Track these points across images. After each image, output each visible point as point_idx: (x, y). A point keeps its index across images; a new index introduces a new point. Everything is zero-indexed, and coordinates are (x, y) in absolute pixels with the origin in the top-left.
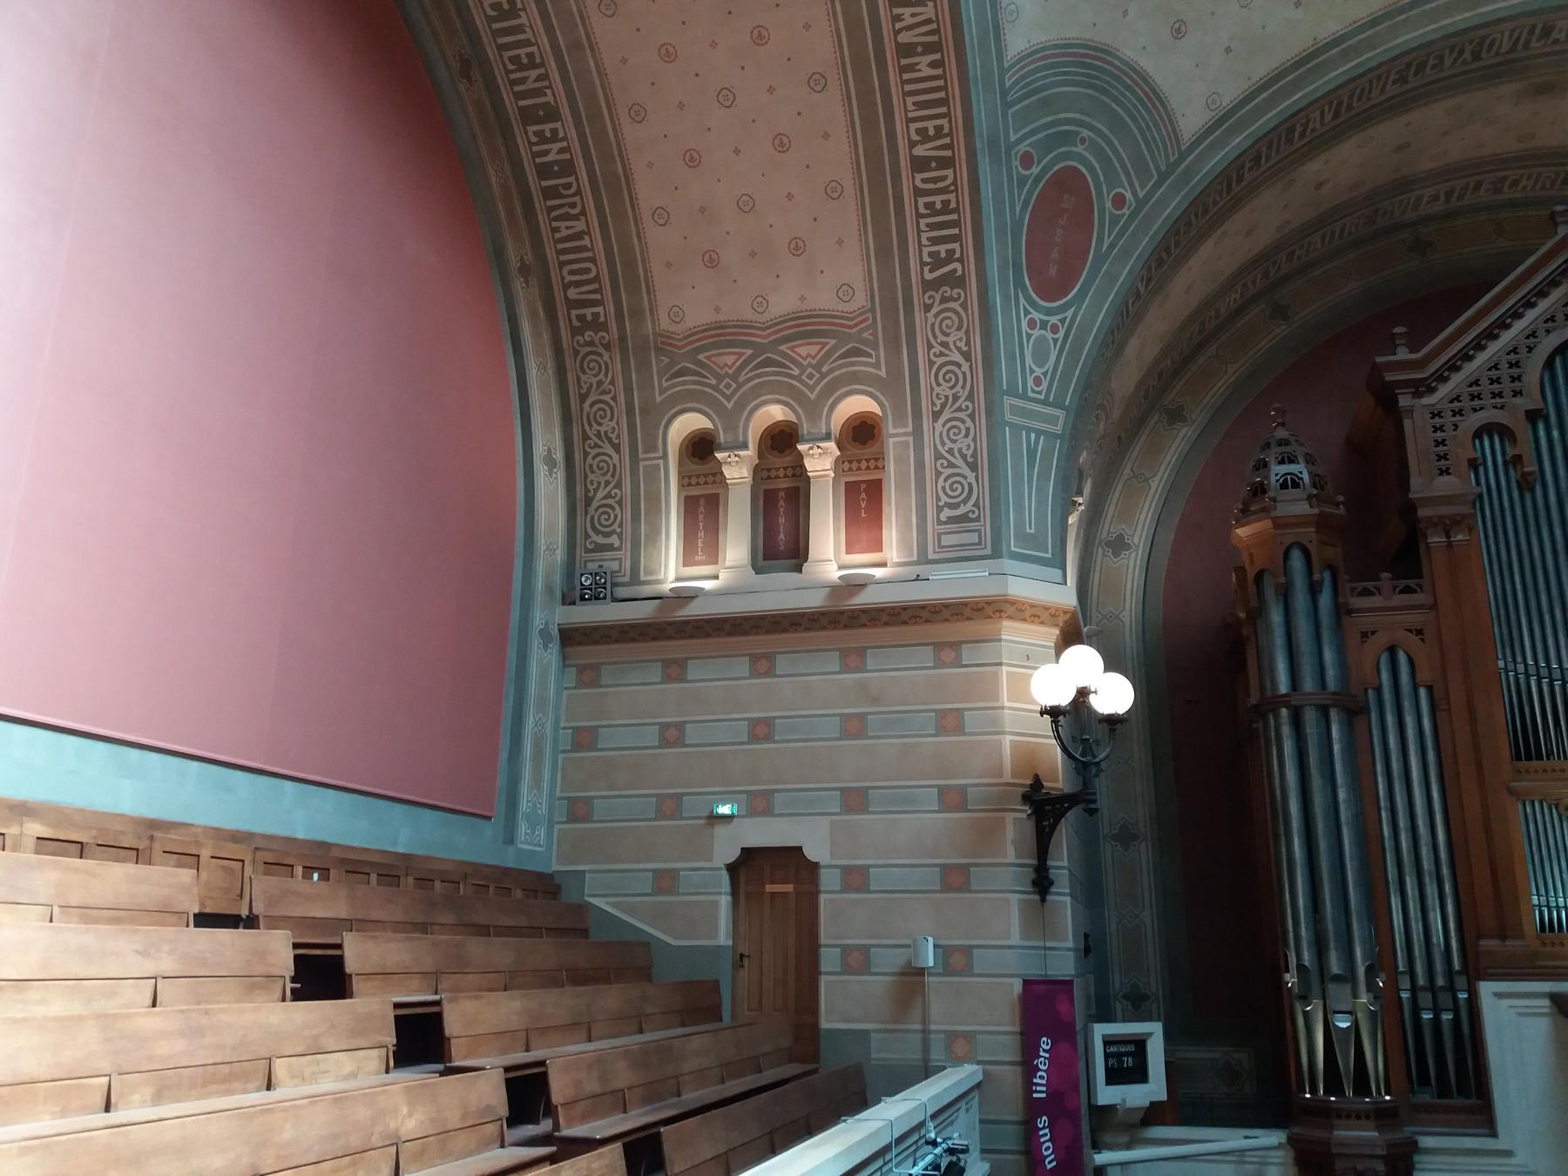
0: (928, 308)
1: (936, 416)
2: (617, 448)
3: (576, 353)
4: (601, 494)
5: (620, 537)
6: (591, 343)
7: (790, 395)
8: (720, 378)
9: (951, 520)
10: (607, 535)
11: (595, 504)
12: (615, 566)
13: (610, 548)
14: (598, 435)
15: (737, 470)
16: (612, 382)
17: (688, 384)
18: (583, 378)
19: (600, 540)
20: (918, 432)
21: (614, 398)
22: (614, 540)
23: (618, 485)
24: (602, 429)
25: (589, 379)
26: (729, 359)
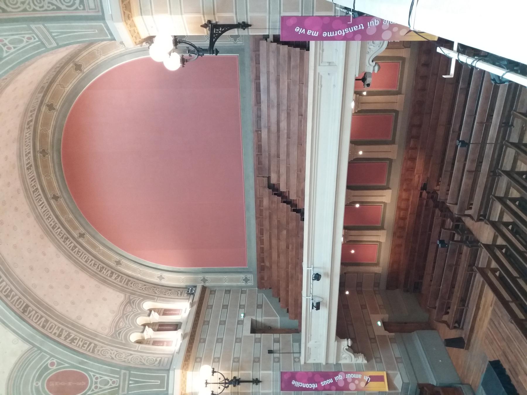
0: (131, 287)
1: (156, 293)
2: (131, 355)
3: (99, 355)
4: (143, 361)
5: (158, 358)
6: (99, 350)
7: (137, 315)
8: (125, 327)
9: (181, 294)
10: (156, 360)
11: (145, 363)
12: (166, 359)
13: (160, 360)
14: (125, 358)
15: (149, 333)
16: (112, 350)
17: (123, 335)
18: (107, 356)
19: (157, 363)
20: (158, 297)
21: (117, 351)
22: (158, 359)
23: (142, 356)
24: (124, 357)
25: (108, 355)
26: (121, 324)
